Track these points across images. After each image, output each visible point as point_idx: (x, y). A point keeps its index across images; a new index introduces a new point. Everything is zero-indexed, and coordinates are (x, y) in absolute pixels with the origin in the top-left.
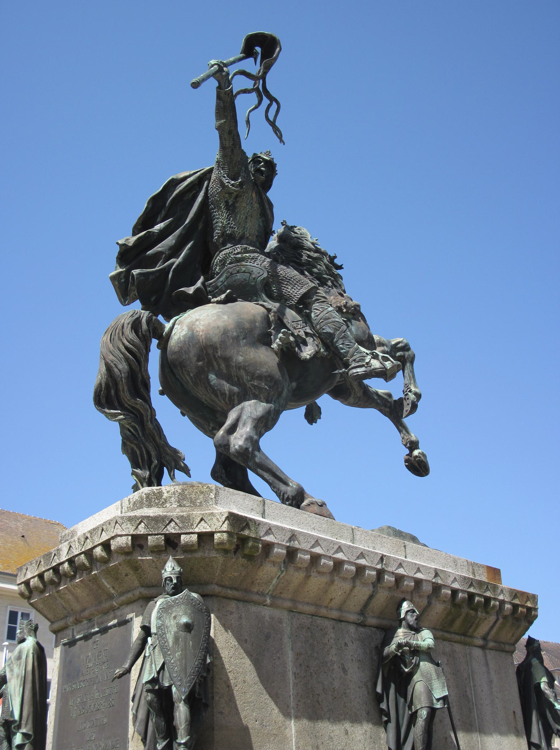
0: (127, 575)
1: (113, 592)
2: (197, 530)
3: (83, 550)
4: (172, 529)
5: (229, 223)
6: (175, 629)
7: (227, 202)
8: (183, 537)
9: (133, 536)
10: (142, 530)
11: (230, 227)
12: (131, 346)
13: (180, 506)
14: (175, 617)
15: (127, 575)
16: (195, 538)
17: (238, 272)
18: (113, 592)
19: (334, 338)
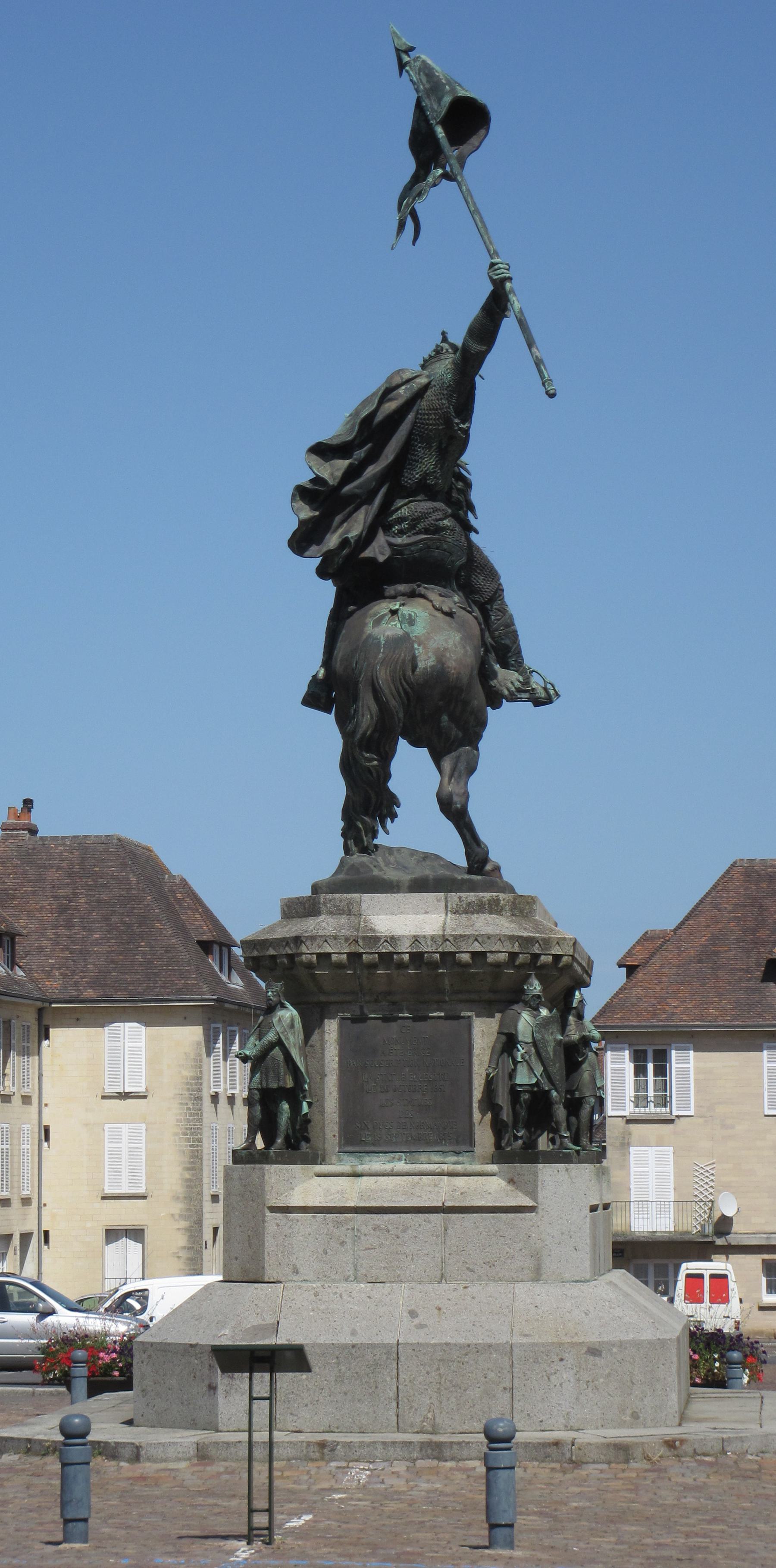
0: (482, 980)
1: (447, 987)
2: (553, 952)
3: (440, 950)
4: (536, 949)
5: (434, 472)
6: (553, 1044)
7: (440, 443)
8: (543, 957)
9: (510, 953)
10: (516, 949)
11: (435, 477)
12: (409, 690)
13: (513, 915)
14: (552, 1033)
15: (482, 980)
16: (550, 958)
17: (437, 548)
18: (447, 987)
19: (509, 651)
